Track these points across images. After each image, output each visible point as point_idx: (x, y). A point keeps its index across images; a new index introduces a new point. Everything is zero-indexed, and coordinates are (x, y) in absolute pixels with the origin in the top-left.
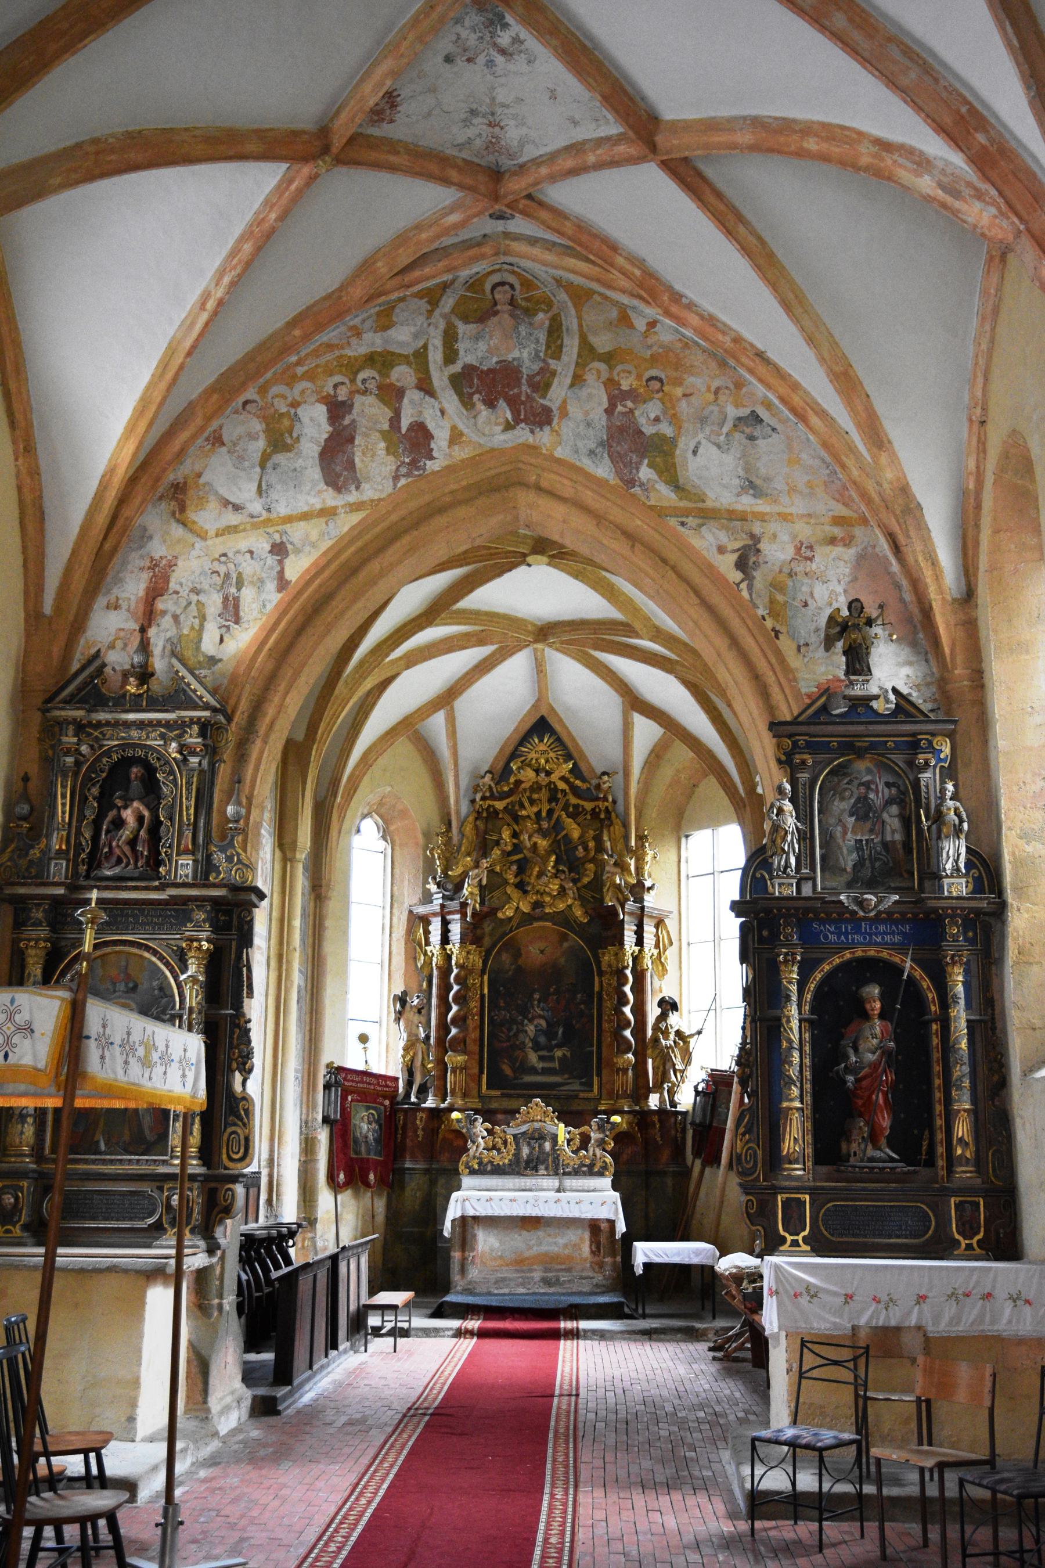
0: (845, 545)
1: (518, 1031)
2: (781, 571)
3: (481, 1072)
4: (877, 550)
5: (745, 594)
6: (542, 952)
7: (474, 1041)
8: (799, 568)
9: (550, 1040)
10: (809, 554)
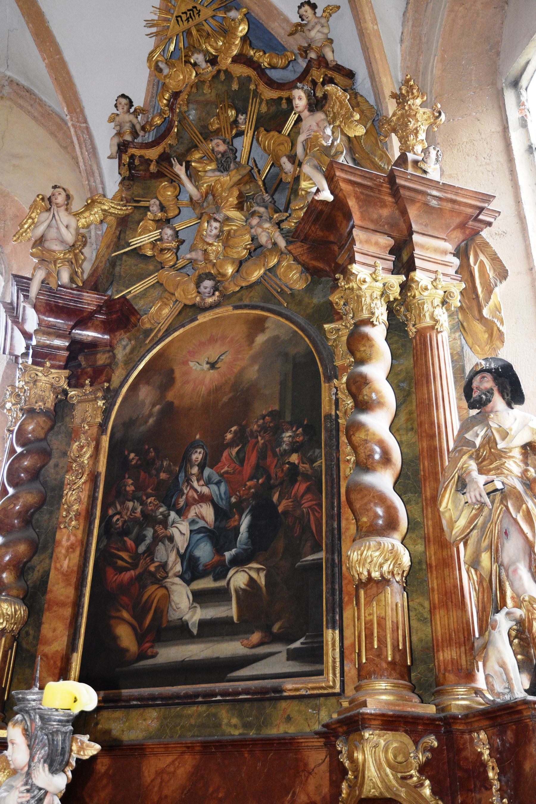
1: (157, 539)
3: (72, 647)
6: (213, 366)
7: (66, 576)
9: (219, 549)
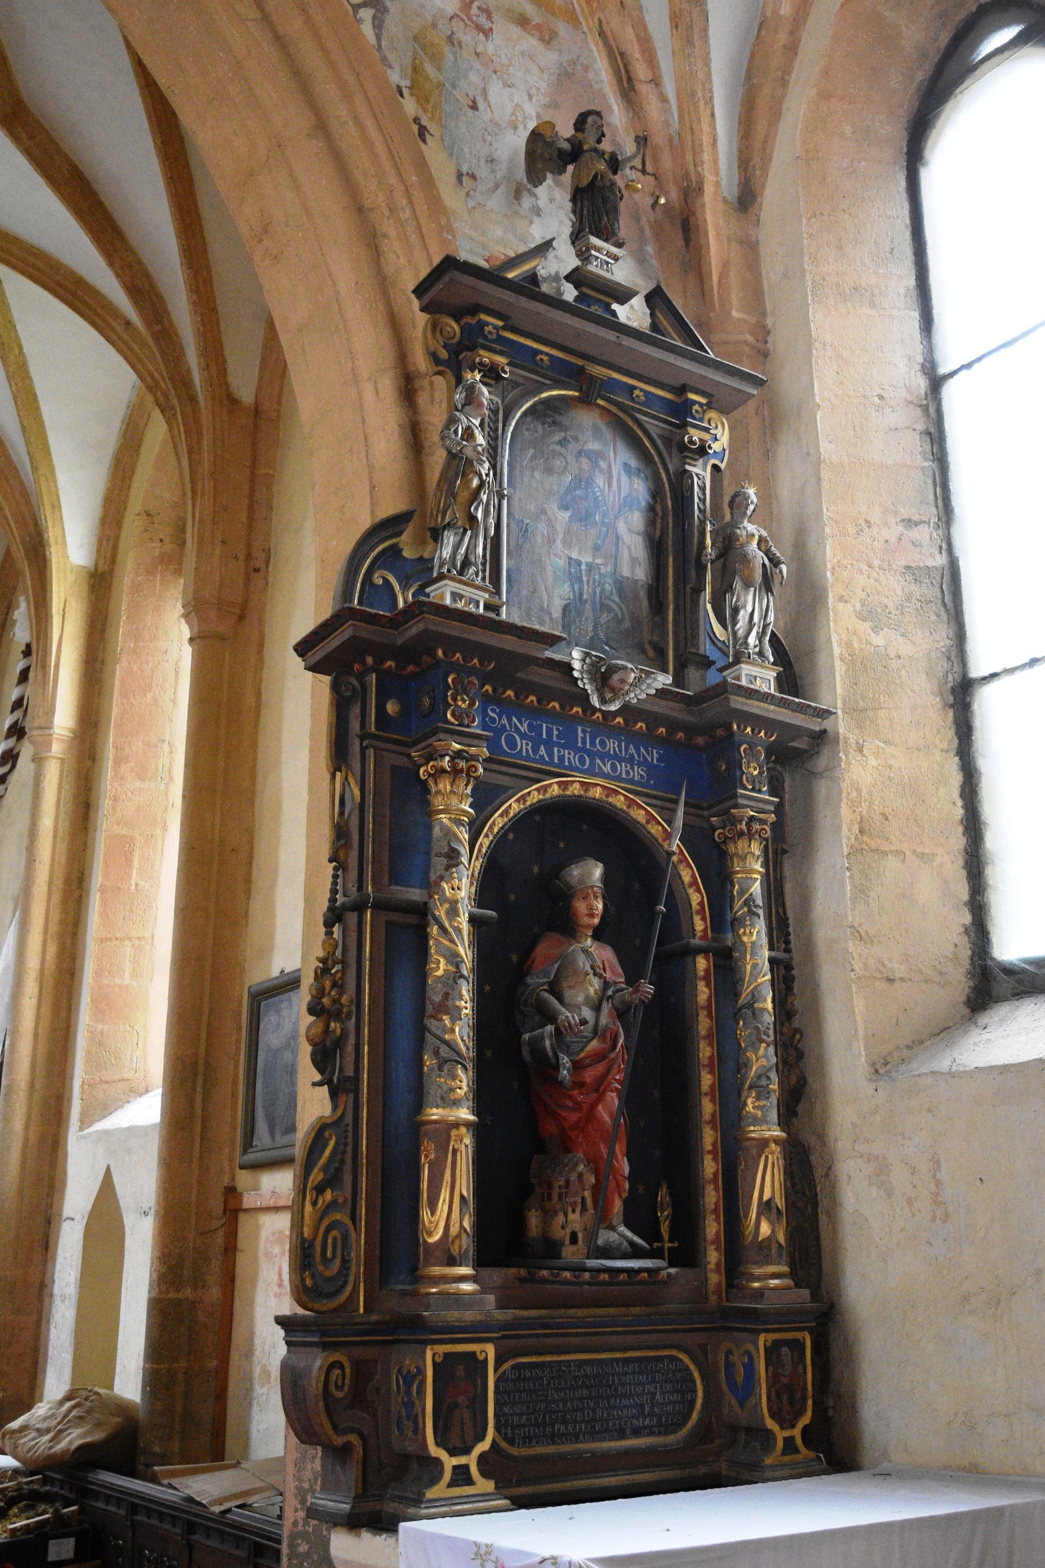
0: (542, 39)
2: (434, 25)
4: (591, 76)
5: (367, 30)
8: (467, 37)
10: (483, 20)
